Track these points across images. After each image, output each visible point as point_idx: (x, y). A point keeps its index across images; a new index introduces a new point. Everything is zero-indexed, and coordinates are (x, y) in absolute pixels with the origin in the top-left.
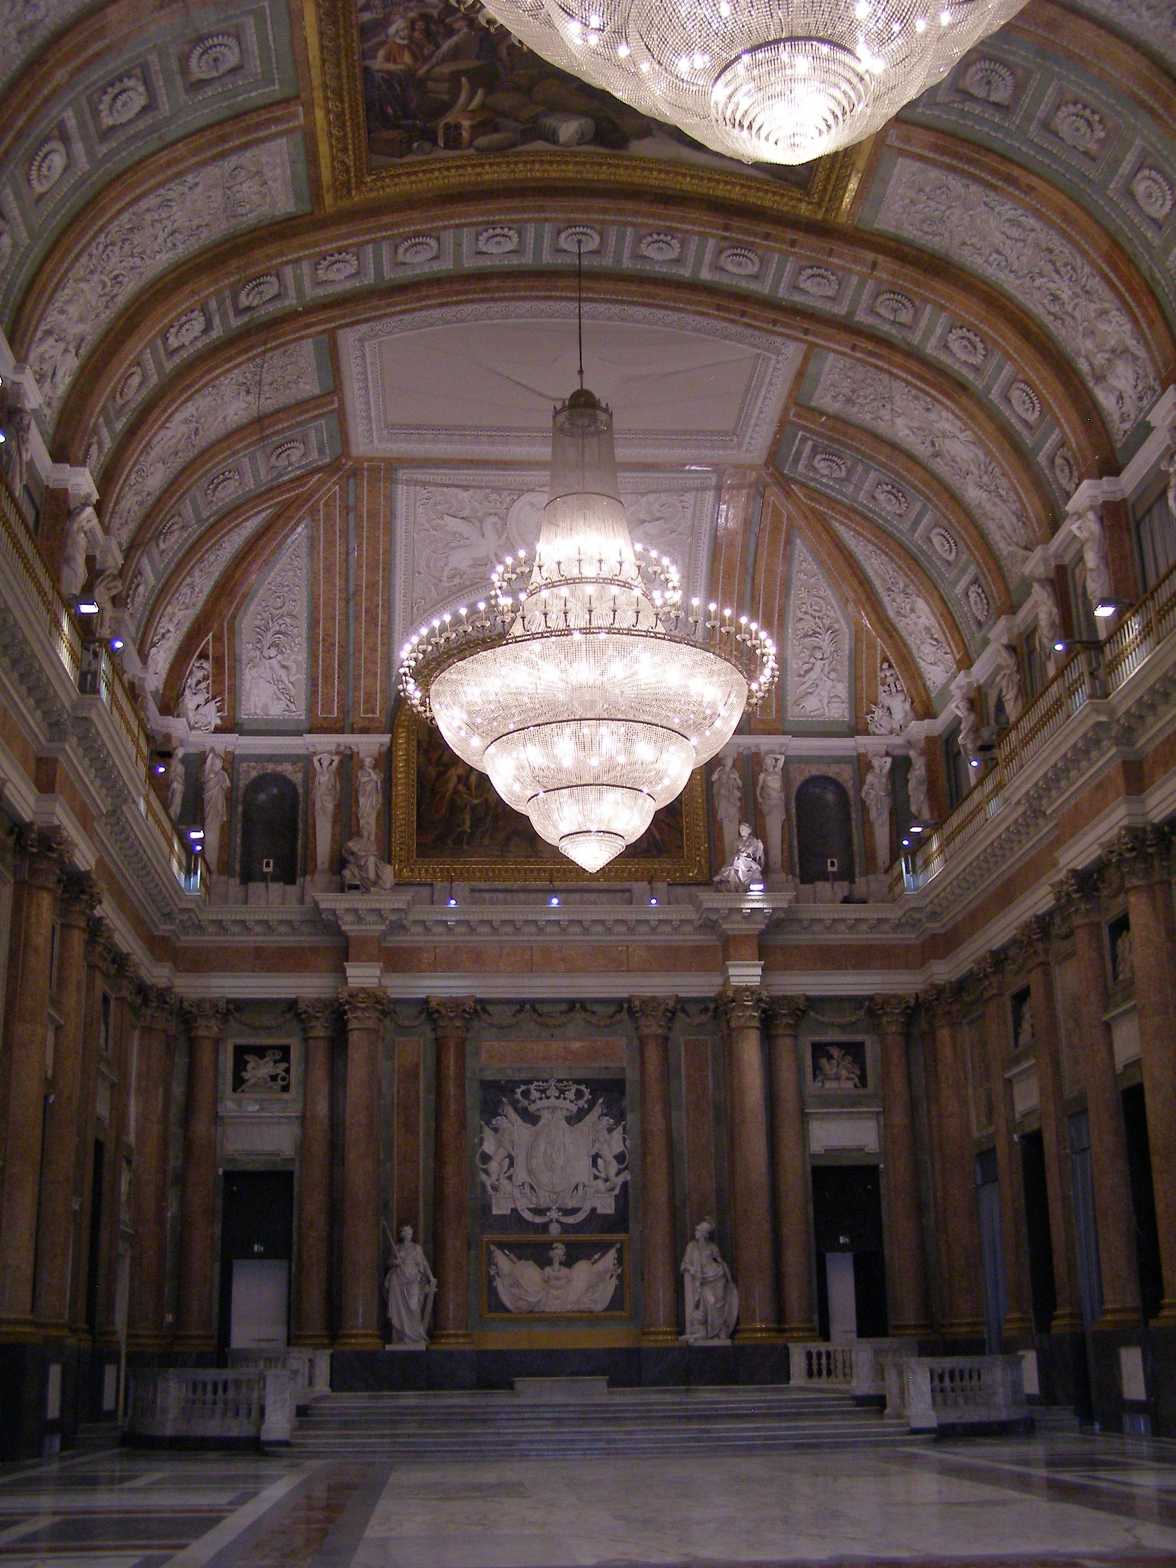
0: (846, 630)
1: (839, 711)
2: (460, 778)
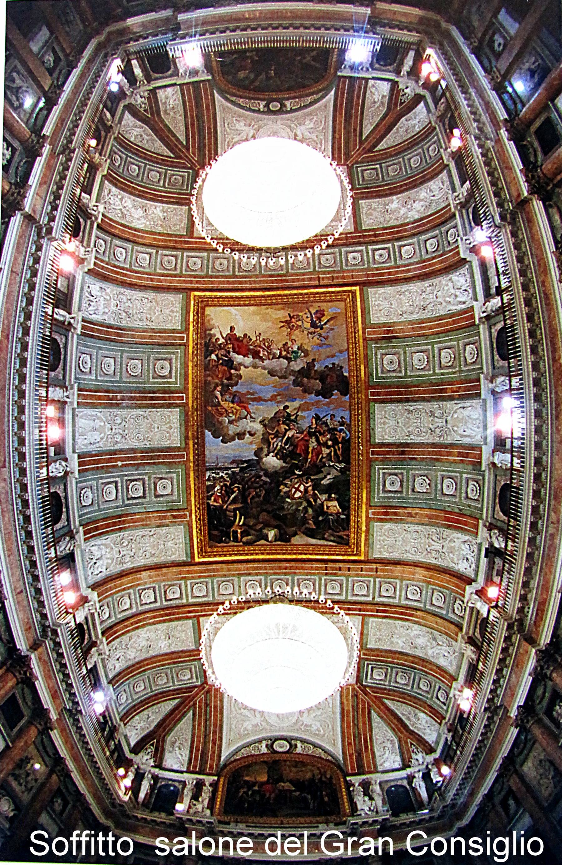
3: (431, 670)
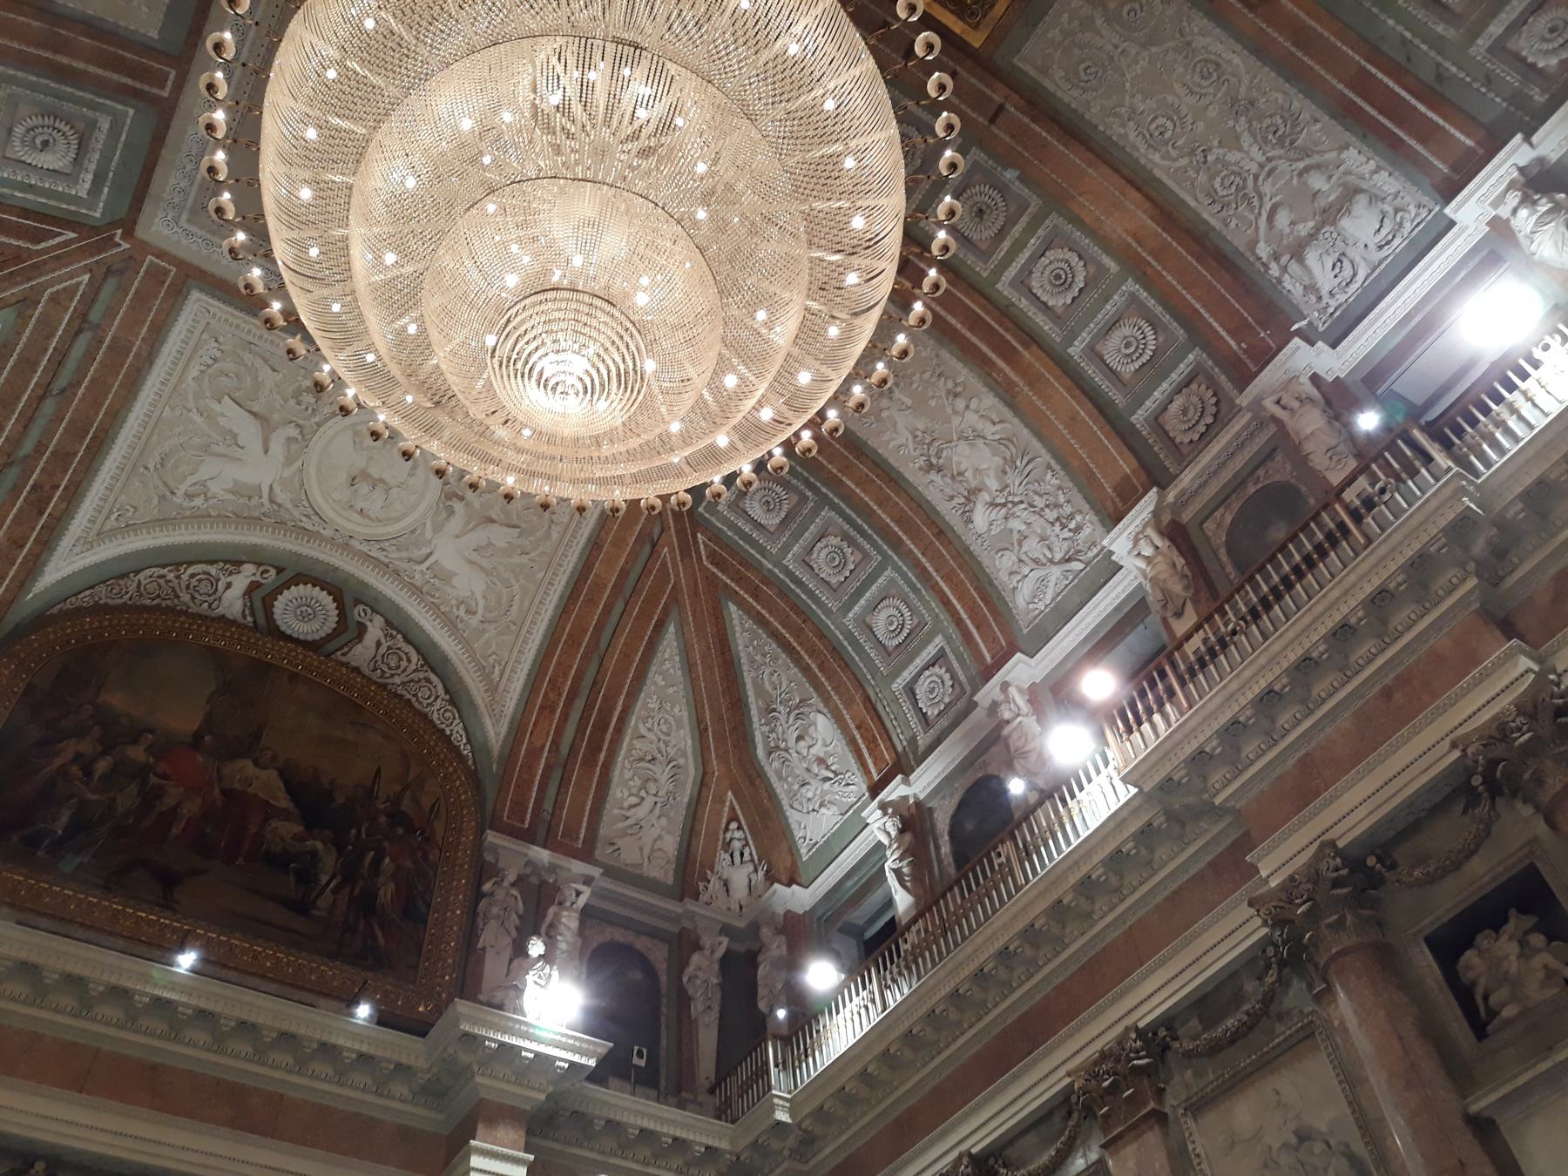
0: (692, 771)
1: (662, 871)
2: (78, 757)
3: (948, 578)
